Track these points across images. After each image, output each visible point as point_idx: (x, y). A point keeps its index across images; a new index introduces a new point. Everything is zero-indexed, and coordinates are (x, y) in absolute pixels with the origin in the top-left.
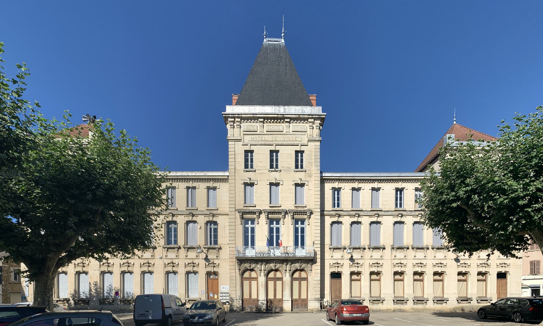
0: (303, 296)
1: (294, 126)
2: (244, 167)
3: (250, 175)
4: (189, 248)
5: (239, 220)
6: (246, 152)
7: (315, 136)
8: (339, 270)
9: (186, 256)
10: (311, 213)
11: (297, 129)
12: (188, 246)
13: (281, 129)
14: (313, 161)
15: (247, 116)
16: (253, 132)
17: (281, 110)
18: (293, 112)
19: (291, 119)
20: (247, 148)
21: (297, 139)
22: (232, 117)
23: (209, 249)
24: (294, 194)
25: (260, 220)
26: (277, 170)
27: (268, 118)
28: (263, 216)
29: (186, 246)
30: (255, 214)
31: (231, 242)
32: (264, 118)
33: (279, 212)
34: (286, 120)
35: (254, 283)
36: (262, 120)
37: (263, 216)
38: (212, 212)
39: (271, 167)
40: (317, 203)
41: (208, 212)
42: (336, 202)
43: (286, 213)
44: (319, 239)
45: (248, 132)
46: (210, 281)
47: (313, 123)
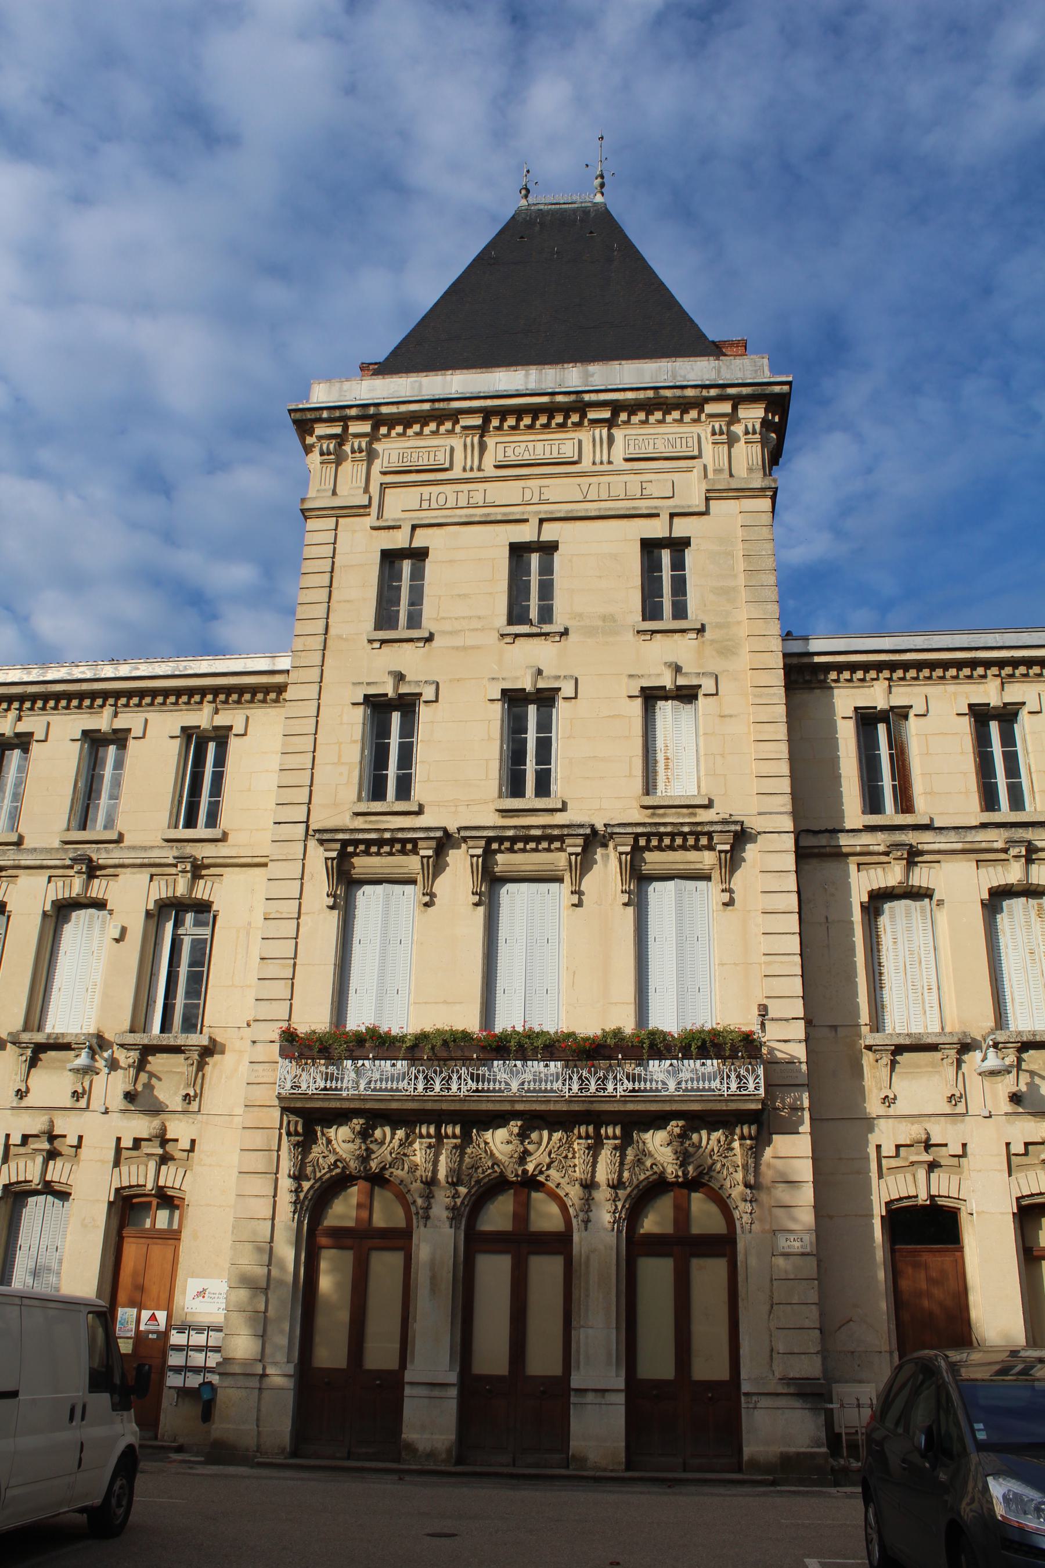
0: (708, 1365)
1: (630, 438)
2: (370, 624)
3: (409, 659)
4: (40, 1049)
5: (319, 886)
6: (390, 558)
7: (741, 469)
8: (943, 1185)
9: (21, 1094)
10: (742, 837)
11: (649, 450)
12: (40, 1038)
13: (568, 451)
14: (741, 580)
15: (403, 408)
16: (433, 474)
17: (571, 377)
18: (629, 381)
19: (617, 407)
20: (399, 540)
21: (651, 490)
22: (330, 420)
23: (147, 1051)
24: (639, 742)
25: (442, 885)
26: (546, 628)
27: (503, 413)
28: (460, 863)
29: (25, 1037)
30: (415, 851)
31: (266, 1011)
32: (487, 414)
33: (551, 839)
34: (592, 415)
35: (385, 1265)
36: (477, 421)
37: (460, 863)
38: (190, 849)
39: (516, 614)
40: (769, 785)
41: (169, 854)
42: (886, 776)
43: (594, 839)
44: (796, 986)
45: (405, 474)
46: (131, 1250)
47: (733, 418)
